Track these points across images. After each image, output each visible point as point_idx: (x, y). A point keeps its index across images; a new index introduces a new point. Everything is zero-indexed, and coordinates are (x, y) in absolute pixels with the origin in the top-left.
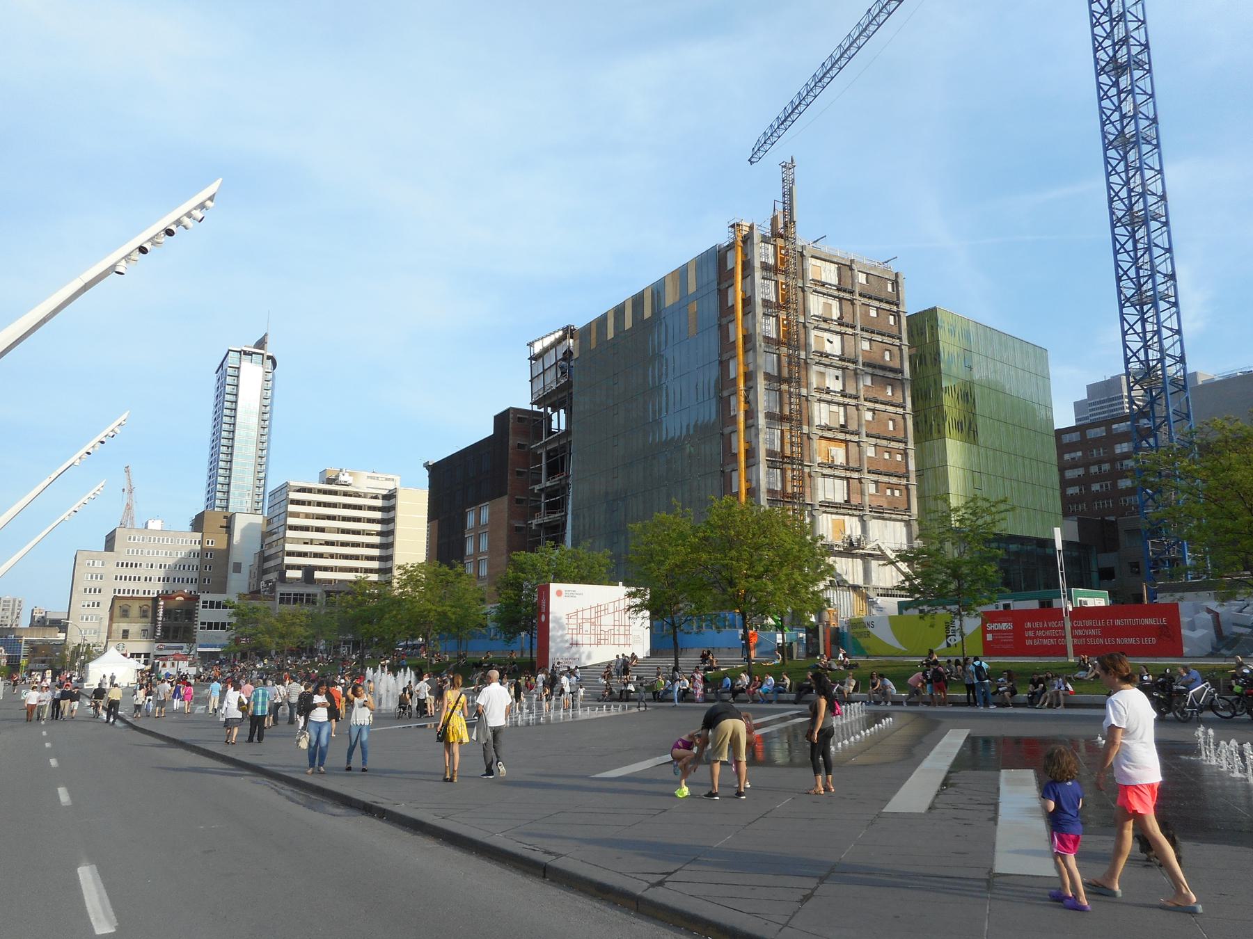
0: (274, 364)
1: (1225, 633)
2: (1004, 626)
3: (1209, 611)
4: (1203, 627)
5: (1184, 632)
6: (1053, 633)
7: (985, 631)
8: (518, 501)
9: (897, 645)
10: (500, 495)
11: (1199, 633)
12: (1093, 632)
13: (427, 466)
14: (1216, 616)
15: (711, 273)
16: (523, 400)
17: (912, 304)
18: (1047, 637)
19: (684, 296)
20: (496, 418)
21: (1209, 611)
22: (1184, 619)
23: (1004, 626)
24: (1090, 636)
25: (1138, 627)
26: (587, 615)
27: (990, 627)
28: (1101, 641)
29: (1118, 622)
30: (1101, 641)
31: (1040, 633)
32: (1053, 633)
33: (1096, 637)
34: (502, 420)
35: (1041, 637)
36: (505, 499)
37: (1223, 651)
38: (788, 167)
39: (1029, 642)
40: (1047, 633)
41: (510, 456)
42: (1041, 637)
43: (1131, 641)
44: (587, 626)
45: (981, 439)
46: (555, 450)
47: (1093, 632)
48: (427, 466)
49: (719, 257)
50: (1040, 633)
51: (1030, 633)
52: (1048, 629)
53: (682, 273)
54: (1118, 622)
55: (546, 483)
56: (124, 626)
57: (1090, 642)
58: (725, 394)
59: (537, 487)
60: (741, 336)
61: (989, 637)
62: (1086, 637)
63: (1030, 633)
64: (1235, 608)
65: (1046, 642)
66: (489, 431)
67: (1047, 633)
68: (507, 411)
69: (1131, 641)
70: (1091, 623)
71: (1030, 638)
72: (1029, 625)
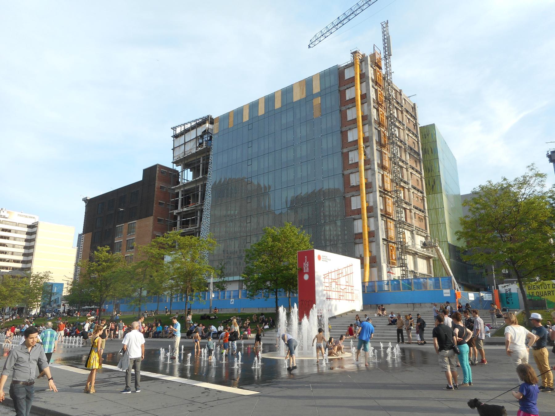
8: (159, 220)
10: (147, 216)
13: (85, 200)
15: (334, 80)
16: (167, 161)
17: (422, 122)
19: (310, 96)
20: (145, 171)
26: (333, 276)
34: (150, 173)
36: (151, 219)
38: (385, 26)
41: (156, 193)
44: (334, 284)
46: (189, 190)
48: (85, 200)
49: (339, 72)
53: (308, 82)
55: (180, 210)
58: (345, 150)
59: (175, 212)
60: (361, 116)
66: (139, 177)
68: (155, 167)
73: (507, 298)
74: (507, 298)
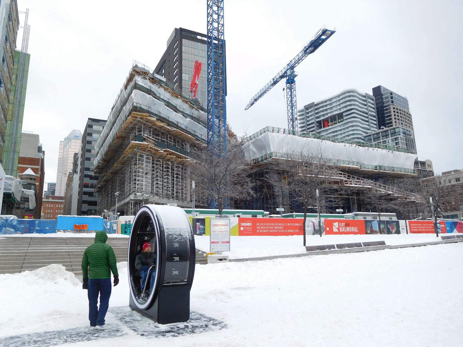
2: (248, 224)
3: (312, 222)
6: (267, 227)
7: (240, 226)
12: (281, 228)
14: (314, 223)
18: (265, 229)
21: (312, 222)
23: (248, 224)
24: (280, 229)
25: (294, 226)
27: (242, 224)
28: (283, 231)
29: (289, 224)
30: (283, 231)
31: (262, 228)
32: (267, 227)
33: (282, 229)
35: (262, 229)
39: (258, 231)
40: (265, 228)
42: (262, 229)
47: (281, 228)
50: (262, 228)
51: (259, 228)
52: (266, 226)
57: (280, 231)
61: (242, 229)
63: (259, 228)
65: (265, 231)
67: (265, 228)
70: (280, 224)
71: (258, 229)
73: (125, 228)
74: (125, 228)
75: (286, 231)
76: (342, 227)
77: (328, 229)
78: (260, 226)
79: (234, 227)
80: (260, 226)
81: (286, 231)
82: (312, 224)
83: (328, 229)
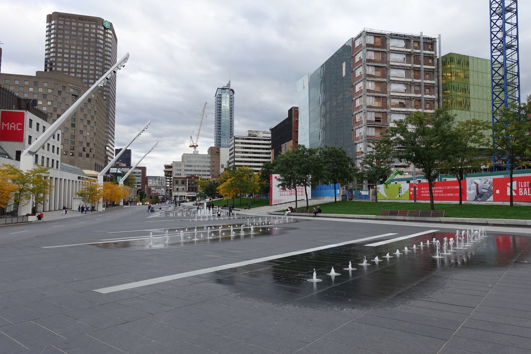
0: (234, 93)
1: (480, 192)
3: (475, 183)
4: (473, 190)
5: (468, 191)
7: (410, 191)
9: (385, 196)
11: (472, 191)
12: (441, 191)
14: (477, 185)
21: (475, 183)
22: (468, 186)
25: (454, 189)
28: (443, 195)
29: (448, 188)
30: (443, 195)
37: (479, 199)
39: (422, 195)
43: (451, 195)
45: (472, 108)
47: (441, 191)
50: (425, 192)
51: (423, 192)
54: (448, 188)
56: (177, 187)
62: (439, 193)
63: (423, 192)
64: (483, 182)
66: (286, 116)
69: (451, 195)
70: (440, 188)
72: (422, 188)
75: (445, 195)
76: (523, 188)
77: (498, 192)
78: (424, 190)
79: (406, 192)
80: (424, 190)
81: (445, 195)
82: (475, 185)
83: (498, 192)
